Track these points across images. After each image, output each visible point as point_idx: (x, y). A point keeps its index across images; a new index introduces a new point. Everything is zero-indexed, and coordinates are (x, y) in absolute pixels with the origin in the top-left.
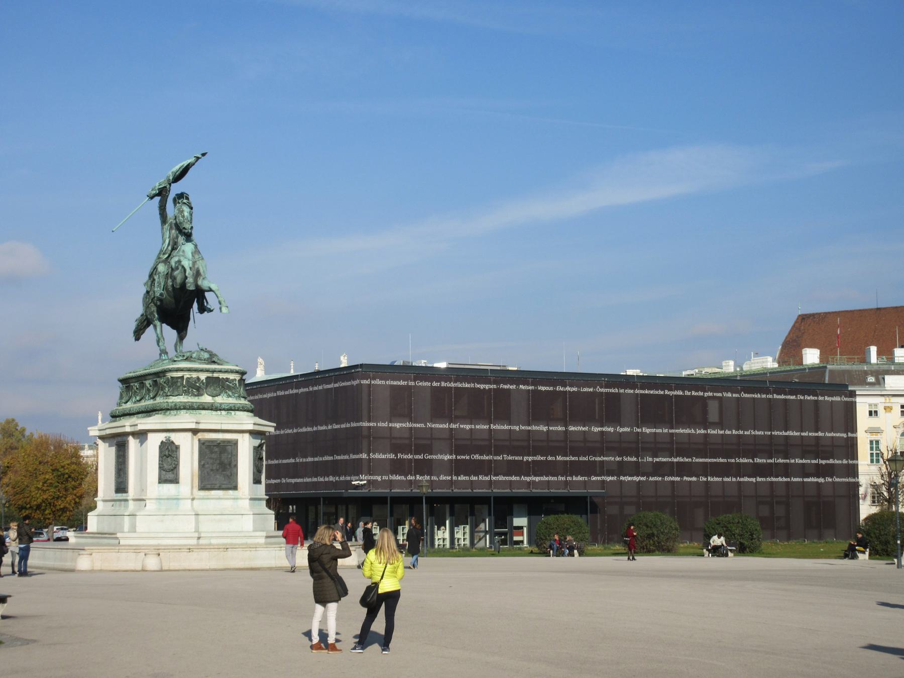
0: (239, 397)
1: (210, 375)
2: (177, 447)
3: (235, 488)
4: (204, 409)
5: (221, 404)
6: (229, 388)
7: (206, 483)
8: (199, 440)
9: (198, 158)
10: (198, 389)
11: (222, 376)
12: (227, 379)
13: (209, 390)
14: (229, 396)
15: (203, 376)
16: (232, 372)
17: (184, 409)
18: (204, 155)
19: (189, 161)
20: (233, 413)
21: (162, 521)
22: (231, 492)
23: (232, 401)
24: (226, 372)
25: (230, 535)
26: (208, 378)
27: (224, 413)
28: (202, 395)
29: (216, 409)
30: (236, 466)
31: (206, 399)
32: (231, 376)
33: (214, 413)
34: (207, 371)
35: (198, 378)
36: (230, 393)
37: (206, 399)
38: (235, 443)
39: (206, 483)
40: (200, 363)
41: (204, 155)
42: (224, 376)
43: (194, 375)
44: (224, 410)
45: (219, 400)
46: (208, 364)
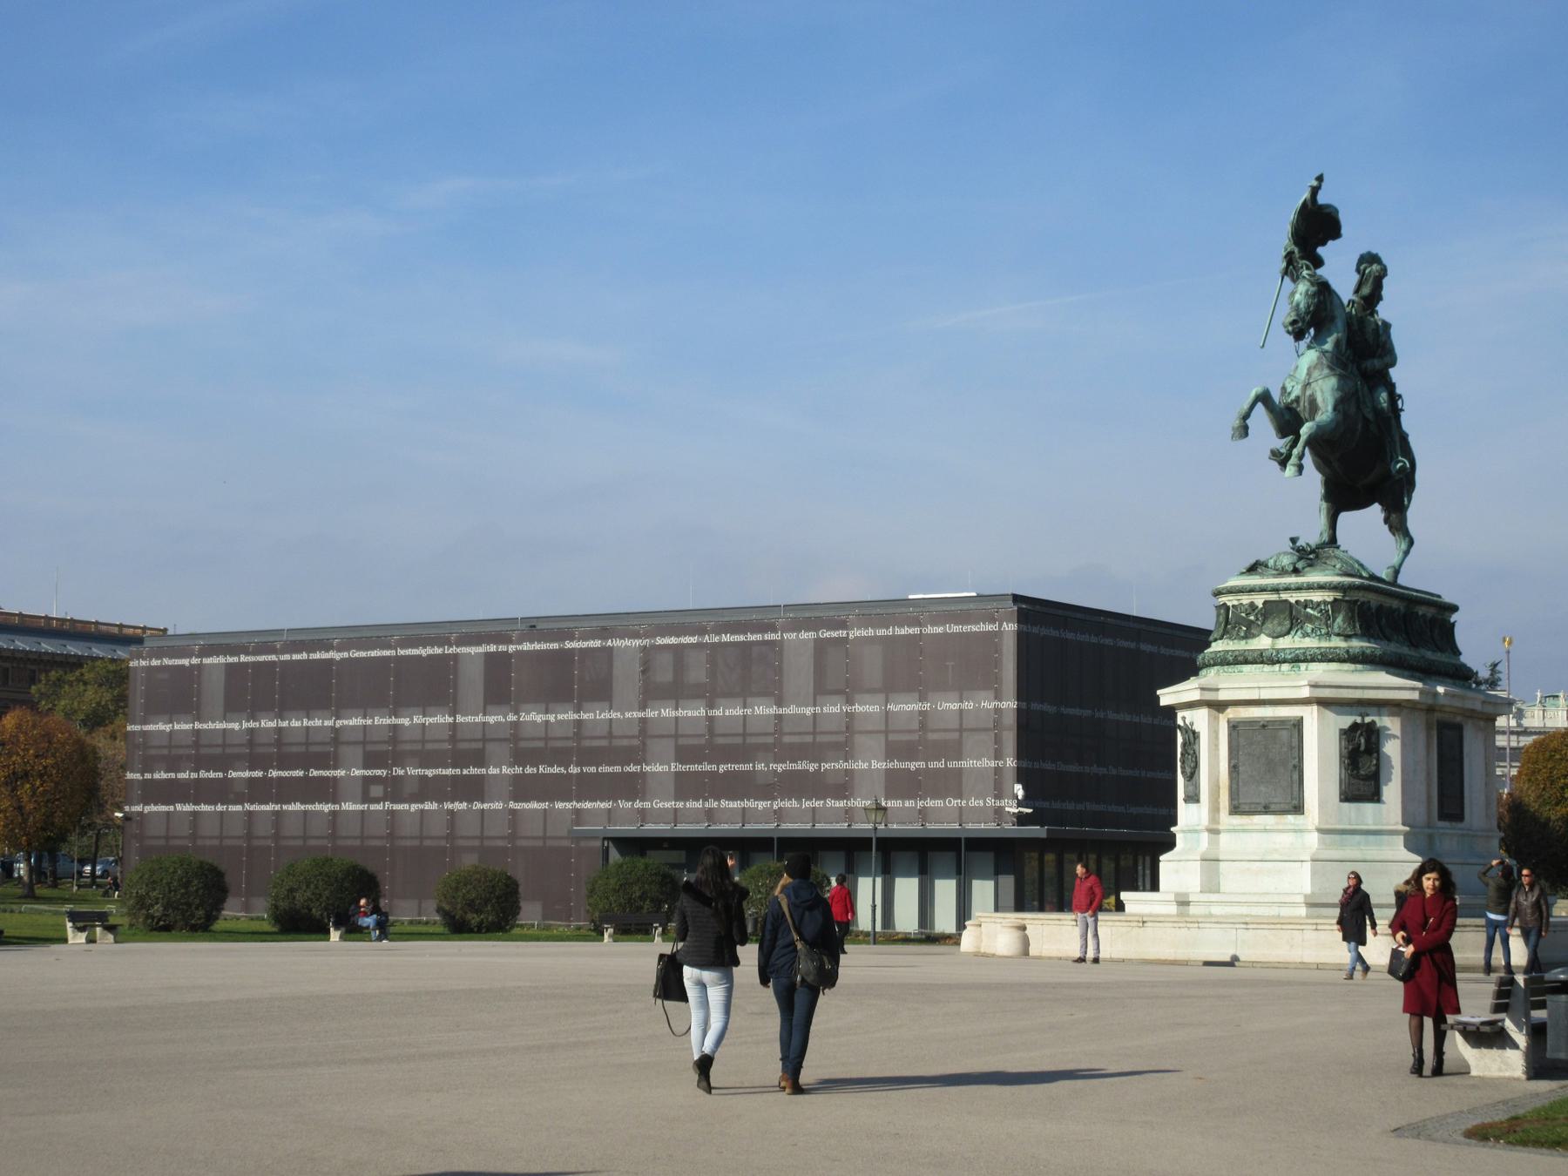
0: (1328, 634)
1: (1274, 597)
3: (1298, 809)
4: (1246, 662)
5: (1278, 651)
10: (1249, 624)
11: (1293, 598)
12: (1306, 604)
13: (1269, 625)
14: (1306, 635)
15: (1259, 600)
16: (1321, 587)
18: (1320, 179)
20: (1303, 666)
22: (1290, 818)
23: (1311, 643)
24: (1299, 588)
25: (1243, 899)
26: (1265, 603)
27: (1285, 667)
28: (1254, 636)
31: (1263, 642)
32: (1317, 597)
33: (1267, 668)
34: (1263, 590)
35: (1252, 605)
36: (1308, 627)
37: (1263, 642)
38: (1298, 724)
40: (1262, 575)
41: (1320, 179)
42: (1302, 596)
43: (1245, 600)
44: (1285, 661)
45: (1285, 643)
46: (1275, 576)
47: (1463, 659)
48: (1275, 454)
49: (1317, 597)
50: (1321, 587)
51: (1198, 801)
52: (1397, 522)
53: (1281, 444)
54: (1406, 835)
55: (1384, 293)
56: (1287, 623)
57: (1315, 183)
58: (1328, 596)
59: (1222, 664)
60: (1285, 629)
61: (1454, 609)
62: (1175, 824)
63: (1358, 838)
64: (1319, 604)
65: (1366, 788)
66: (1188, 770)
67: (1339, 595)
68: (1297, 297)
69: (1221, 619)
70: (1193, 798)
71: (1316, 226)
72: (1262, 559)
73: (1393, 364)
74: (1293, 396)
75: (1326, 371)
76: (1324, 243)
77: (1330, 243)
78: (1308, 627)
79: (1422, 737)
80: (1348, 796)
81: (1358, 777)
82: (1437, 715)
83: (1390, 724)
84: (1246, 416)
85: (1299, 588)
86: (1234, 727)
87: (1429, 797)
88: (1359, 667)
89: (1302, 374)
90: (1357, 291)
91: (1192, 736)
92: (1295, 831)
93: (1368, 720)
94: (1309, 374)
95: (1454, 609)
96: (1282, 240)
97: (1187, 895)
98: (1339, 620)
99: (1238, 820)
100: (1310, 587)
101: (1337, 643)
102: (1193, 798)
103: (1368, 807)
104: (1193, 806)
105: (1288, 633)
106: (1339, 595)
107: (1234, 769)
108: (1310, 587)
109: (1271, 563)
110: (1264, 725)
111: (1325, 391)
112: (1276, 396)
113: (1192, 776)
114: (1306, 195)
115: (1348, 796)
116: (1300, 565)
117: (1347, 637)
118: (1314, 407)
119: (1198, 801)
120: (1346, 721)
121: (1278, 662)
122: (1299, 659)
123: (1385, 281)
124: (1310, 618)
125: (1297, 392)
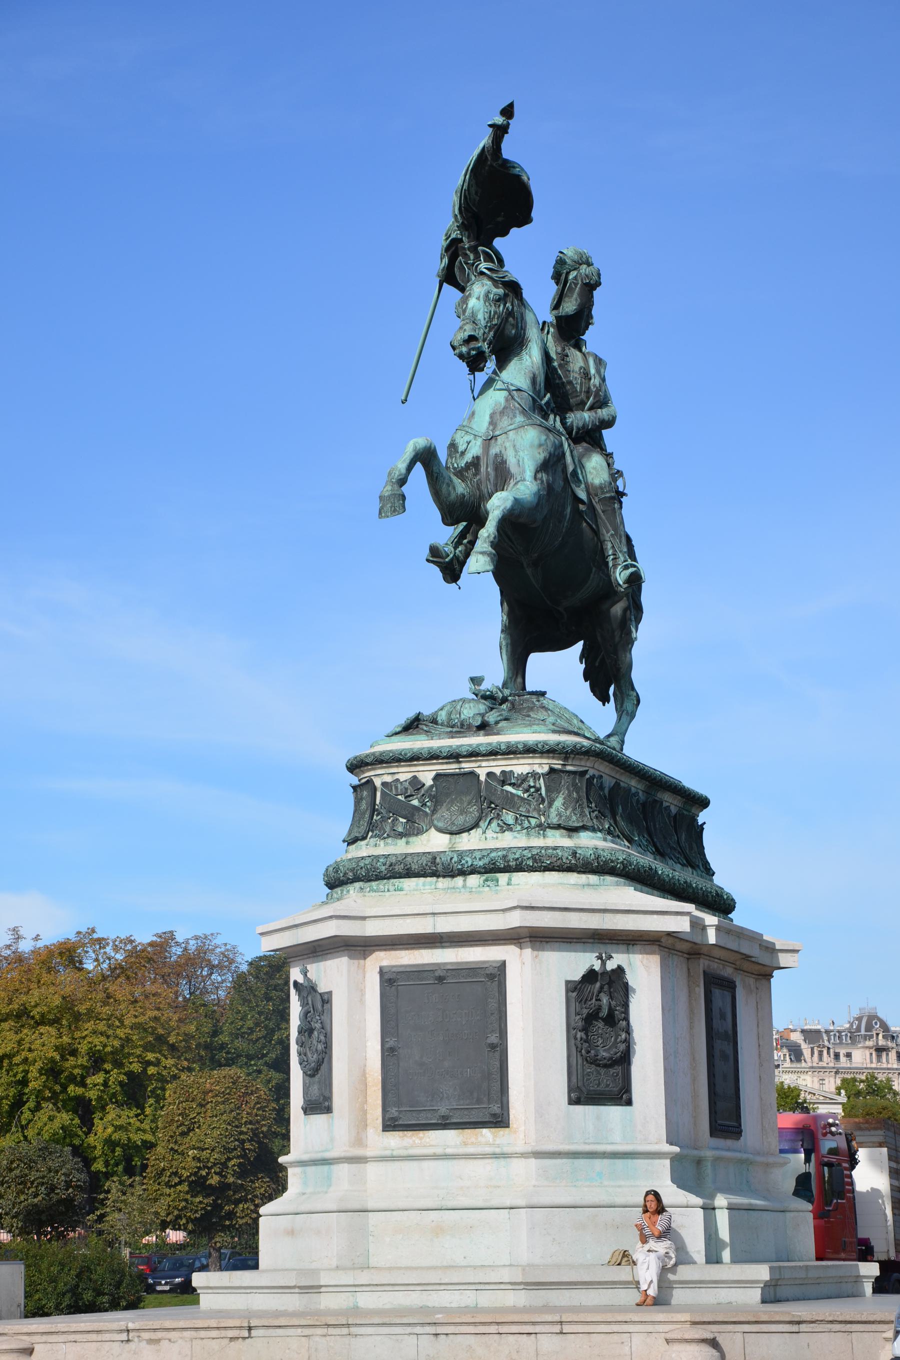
1: (451, 768)
2: (326, 1000)
3: (500, 1121)
4: (409, 874)
5: (461, 854)
6: (510, 802)
7: (404, 1111)
8: (382, 972)
9: (500, 131)
10: (411, 815)
11: (483, 769)
12: (505, 778)
14: (506, 828)
15: (427, 774)
17: (356, 879)
18: (508, 112)
19: (481, 145)
20: (503, 878)
21: (291, 1232)
22: (486, 1133)
23: (514, 841)
24: (493, 753)
26: (437, 777)
27: (474, 880)
28: (420, 832)
29: (450, 872)
30: (500, 1049)
31: (433, 842)
32: (520, 767)
33: (443, 883)
34: (433, 756)
35: (415, 783)
36: (509, 818)
37: (433, 842)
38: (496, 975)
39: (404, 1111)
41: (508, 112)
42: (498, 766)
44: (473, 871)
45: (470, 841)
46: (452, 735)
47: (718, 880)
48: (435, 553)
49: (520, 767)
50: (529, 750)
51: (328, 1110)
52: (608, 674)
53: (444, 535)
54: (675, 1160)
55: (594, 312)
56: (474, 810)
57: (499, 120)
58: (540, 766)
59: (368, 879)
60: (470, 819)
61: (704, 803)
62: (285, 1149)
63: (598, 1163)
64: (524, 778)
65: (606, 1080)
66: (313, 1058)
67: (557, 764)
68: (472, 303)
69: (364, 805)
70: (319, 1104)
71: (496, 199)
72: (427, 712)
73: (609, 423)
74: (468, 457)
75: (520, 419)
76: (504, 233)
77: (514, 231)
78: (509, 817)
79: (683, 997)
80: (582, 1094)
81: (595, 1062)
82: (703, 963)
83: (644, 975)
84: (402, 482)
85: (493, 753)
86: (390, 980)
87: (695, 1095)
88: (593, 879)
89: (481, 424)
90: (556, 306)
91: (319, 1004)
92: (496, 1156)
93: (611, 965)
94: (493, 423)
95: (704, 803)
96: (442, 218)
97: (315, 1272)
98: (559, 803)
99: (397, 1141)
100: (511, 751)
101: (557, 840)
102: (319, 1104)
103: (613, 1113)
104: (319, 1120)
105: (476, 825)
106: (557, 764)
107: (389, 1053)
108: (511, 751)
109: (442, 716)
110: (440, 977)
111: (525, 448)
112: (442, 455)
113: (319, 1068)
114: (485, 140)
115: (582, 1094)
116: (491, 717)
117: (572, 830)
118: (503, 475)
119: (328, 1110)
120: (578, 963)
121: (463, 873)
122: (496, 867)
123: (596, 293)
124: (510, 802)
125: (476, 449)
